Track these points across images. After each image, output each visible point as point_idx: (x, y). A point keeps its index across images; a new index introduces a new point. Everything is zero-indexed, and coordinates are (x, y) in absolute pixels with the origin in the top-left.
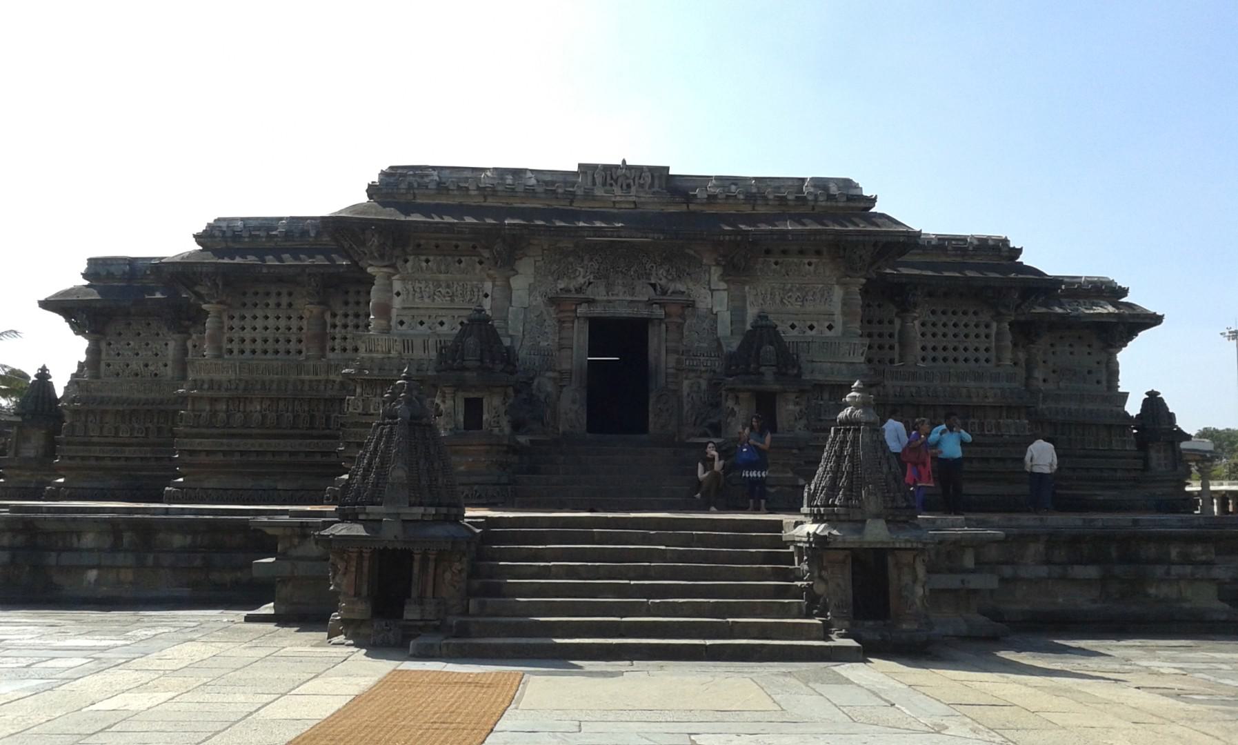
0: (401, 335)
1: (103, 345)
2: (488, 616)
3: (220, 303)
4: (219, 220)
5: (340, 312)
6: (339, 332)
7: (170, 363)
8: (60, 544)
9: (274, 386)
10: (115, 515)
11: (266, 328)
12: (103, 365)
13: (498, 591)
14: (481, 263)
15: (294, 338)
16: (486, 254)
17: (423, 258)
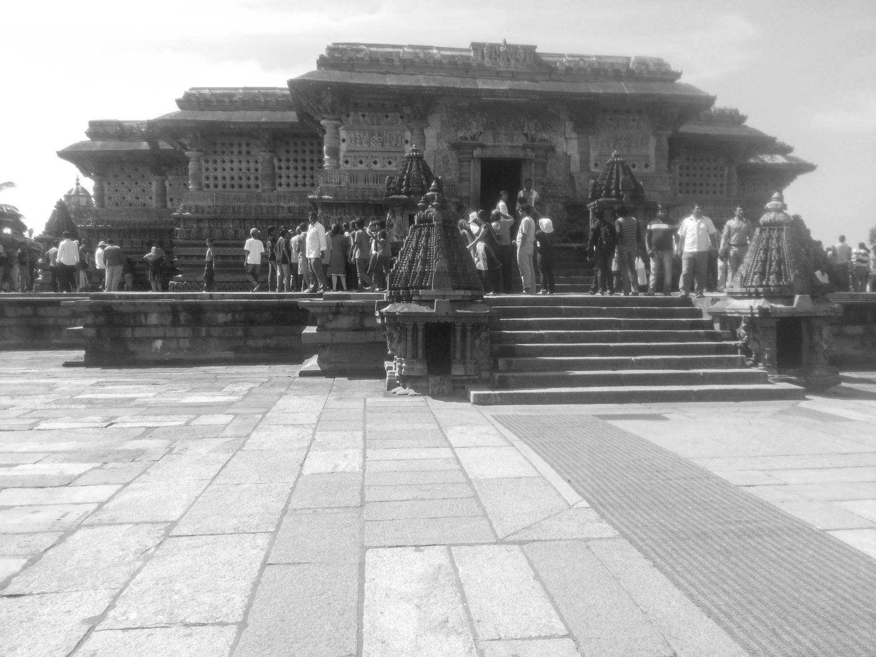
0: (349, 171)
1: (105, 185)
2: (515, 371)
3: (197, 150)
4: (193, 89)
5: (283, 158)
6: (284, 172)
7: (154, 197)
8: (132, 322)
9: (242, 210)
10: (174, 300)
11: (232, 169)
12: (106, 198)
13: (510, 352)
14: (402, 117)
15: (252, 177)
16: (407, 110)
17: (361, 113)
